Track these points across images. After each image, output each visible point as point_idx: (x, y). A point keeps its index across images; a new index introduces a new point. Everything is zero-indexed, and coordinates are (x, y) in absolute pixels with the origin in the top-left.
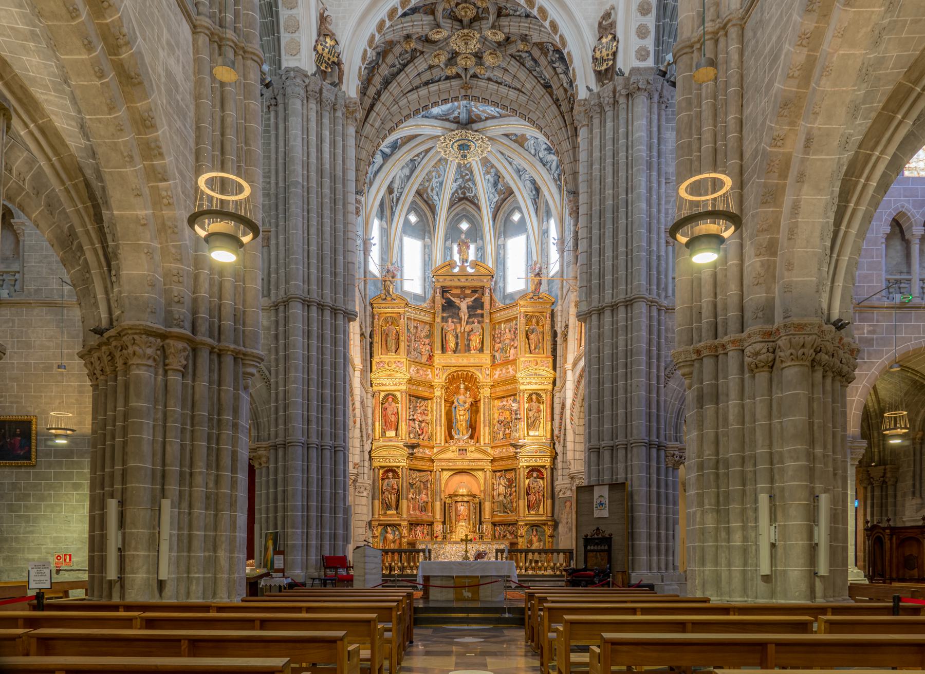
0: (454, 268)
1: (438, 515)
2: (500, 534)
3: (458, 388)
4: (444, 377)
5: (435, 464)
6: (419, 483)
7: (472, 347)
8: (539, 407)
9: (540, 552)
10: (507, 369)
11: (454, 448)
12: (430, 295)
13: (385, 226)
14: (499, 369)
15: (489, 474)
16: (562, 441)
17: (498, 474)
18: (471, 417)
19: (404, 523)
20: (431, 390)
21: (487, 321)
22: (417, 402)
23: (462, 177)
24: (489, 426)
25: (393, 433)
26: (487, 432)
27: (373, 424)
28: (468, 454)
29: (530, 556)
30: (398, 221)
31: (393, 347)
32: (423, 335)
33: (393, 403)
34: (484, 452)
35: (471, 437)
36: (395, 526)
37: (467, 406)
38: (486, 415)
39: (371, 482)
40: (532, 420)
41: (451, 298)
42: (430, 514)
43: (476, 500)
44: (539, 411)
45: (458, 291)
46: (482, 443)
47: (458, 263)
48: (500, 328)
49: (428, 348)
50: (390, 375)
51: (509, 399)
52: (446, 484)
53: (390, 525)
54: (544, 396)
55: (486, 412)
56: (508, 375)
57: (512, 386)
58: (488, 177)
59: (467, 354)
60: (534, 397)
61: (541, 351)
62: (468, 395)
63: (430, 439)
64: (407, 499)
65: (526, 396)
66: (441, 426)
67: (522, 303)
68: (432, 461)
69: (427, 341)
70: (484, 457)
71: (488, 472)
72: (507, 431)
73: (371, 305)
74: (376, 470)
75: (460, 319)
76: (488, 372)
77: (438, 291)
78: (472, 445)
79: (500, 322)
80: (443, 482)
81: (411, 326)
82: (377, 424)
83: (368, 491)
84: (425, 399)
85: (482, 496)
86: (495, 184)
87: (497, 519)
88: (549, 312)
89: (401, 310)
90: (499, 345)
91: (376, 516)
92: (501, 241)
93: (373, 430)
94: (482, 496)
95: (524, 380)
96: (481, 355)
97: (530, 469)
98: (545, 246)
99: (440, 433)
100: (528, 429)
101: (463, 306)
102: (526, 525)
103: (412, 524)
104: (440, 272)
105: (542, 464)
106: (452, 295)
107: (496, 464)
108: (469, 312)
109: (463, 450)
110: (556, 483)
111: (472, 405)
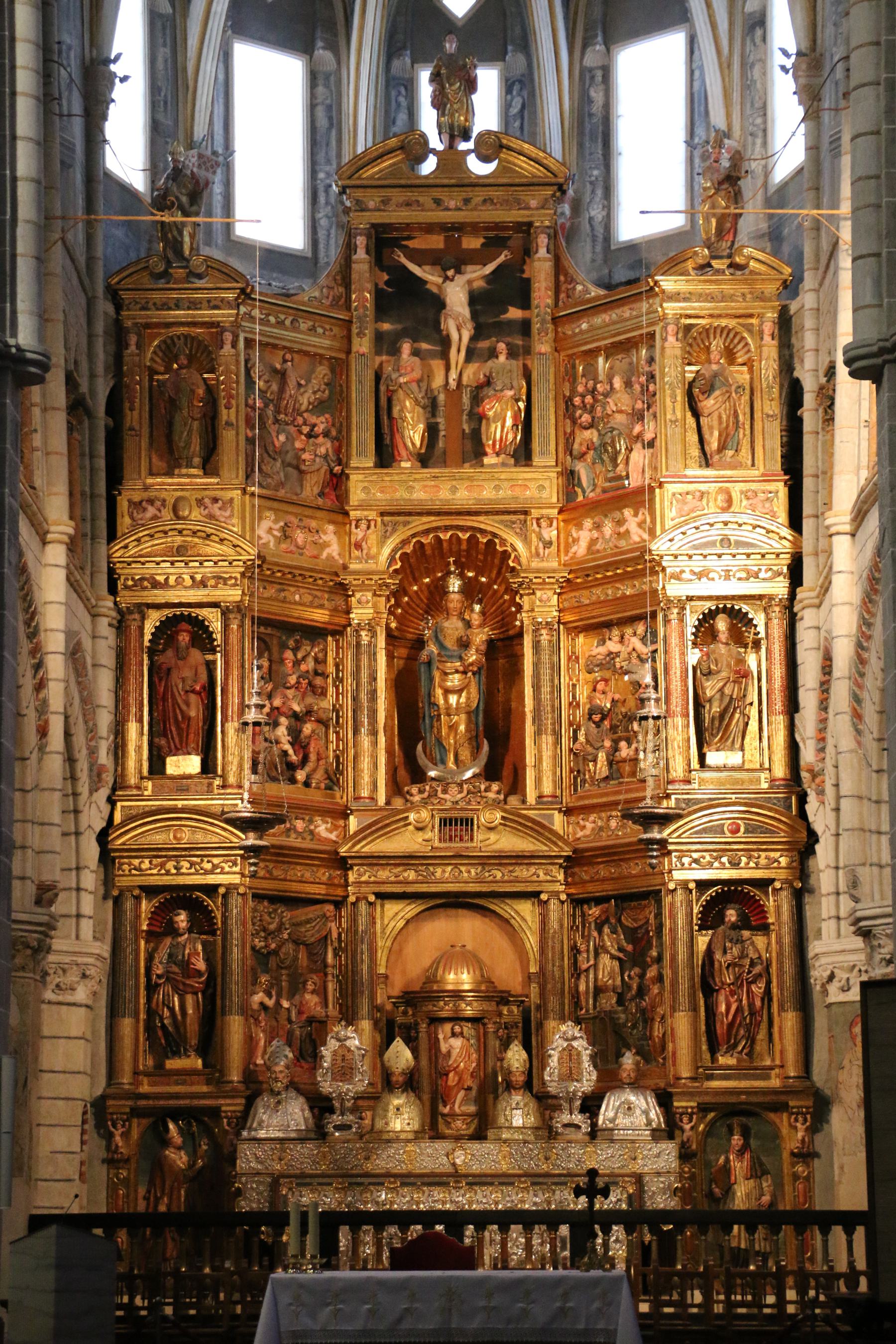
0: (422, 159)
3: (439, 591)
4: (386, 551)
5: (352, 877)
6: (290, 947)
8: (741, 661)
10: (620, 522)
11: (425, 814)
12: (331, 253)
14: (588, 523)
16: (830, 791)
17: (594, 911)
18: (489, 695)
20: (340, 602)
22: (283, 646)
25: (191, 764)
26: (547, 754)
28: (479, 836)
31: (196, 446)
33: (196, 656)
34: (539, 829)
35: (491, 773)
37: (472, 657)
38: (546, 689)
39: (105, 949)
40: (716, 709)
44: (743, 675)
45: (437, 242)
46: (531, 796)
47: (436, 143)
48: (591, 373)
49: (325, 446)
50: (181, 551)
51: (629, 631)
52: (396, 952)
53: (176, 1114)
54: (759, 619)
55: (545, 678)
56: (622, 543)
59: (467, 470)
60: (722, 624)
61: (745, 451)
63: (333, 780)
64: (245, 1011)
65: (691, 620)
66: (374, 733)
67: (668, 283)
68: (343, 864)
69: (321, 423)
71: (553, 905)
72: (625, 751)
73: (113, 294)
74: (129, 904)
75: (446, 342)
76: (551, 534)
77: (361, 241)
78: (496, 804)
79: (593, 353)
80: (382, 944)
82: (132, 728)
83: (92, 984)
88: (772, 315)
89: (224, 315)
90: (587, 434)
91: (126, 1079)
92: (592, 58)
93: (119, 749)
95: (683, 562)
96: (523, 473)
97: (712, 891)
100: (701, 744)
102: (703, 1109)
107: (584, 873)
108: (474, 315)
110: (814, 948)
111: (491, 648)
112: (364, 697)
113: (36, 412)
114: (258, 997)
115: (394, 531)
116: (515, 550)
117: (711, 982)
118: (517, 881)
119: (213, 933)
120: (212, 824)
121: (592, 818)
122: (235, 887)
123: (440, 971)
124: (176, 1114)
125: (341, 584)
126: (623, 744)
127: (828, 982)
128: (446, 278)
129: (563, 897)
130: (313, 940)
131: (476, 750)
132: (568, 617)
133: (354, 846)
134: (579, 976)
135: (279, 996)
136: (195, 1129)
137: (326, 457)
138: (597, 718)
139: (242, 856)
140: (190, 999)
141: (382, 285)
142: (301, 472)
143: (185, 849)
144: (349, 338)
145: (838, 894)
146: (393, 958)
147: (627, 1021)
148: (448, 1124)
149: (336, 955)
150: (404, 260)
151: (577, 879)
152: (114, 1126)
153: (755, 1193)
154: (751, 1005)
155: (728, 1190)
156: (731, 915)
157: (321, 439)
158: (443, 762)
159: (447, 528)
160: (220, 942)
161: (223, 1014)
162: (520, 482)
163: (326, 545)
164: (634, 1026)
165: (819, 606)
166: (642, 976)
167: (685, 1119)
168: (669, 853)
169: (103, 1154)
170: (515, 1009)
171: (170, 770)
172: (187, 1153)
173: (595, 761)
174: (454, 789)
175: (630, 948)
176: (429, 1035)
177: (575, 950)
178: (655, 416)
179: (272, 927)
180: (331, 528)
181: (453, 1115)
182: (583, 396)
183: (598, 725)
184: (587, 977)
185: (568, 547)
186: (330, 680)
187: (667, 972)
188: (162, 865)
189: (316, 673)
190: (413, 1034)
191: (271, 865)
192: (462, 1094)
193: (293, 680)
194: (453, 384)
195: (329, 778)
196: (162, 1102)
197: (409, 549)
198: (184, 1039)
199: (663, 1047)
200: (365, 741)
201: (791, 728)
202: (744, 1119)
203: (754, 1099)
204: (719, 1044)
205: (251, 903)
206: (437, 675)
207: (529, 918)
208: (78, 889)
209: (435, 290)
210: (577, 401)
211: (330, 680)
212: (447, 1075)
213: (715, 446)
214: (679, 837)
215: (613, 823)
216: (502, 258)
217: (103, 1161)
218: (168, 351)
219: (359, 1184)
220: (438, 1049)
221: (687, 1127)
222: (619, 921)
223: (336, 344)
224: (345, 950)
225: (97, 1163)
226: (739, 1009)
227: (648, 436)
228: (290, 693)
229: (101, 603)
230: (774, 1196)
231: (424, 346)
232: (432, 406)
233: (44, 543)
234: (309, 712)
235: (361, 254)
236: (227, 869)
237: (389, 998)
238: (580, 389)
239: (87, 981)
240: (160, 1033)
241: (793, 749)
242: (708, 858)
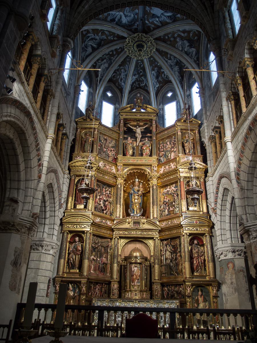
1: (115, 276)
2: (168, 294)
5: (114, 233)
7: (144, 154)
9: (208, 312)
13: (92, 91)
14: (163, 167)
15: (158, 242)
17: (165, 242)
19: (84, 281)
21: (154, 138)
22: (103, 187)
23: (139, 74)
24: (157, 205)
25: (82, 206)
27: (67, 200)
29: (198, 316)
30: (100, 90)
32: (110, 145)
34: (154, 224)
35: (143, 215)
36: (77, 284)
37: (140, 193)
38: (155, 197)
39: (59, 244)
41: (132, 127)
42: (108, 274)
43: (147, 263)
45: (135, 123)
46: (152, 218)
49: (114, 153)
51: (172, 186)
53: (71, 282)
56: (170, 169)
57: (174, 176)
58: (153, 72)
62: (141, 186)
63: (111, 214)
64: (89, 259)
68: (112, 230)
70: (155, 228)
71: (157, 239)
72: (171, 209)
74: (65, 234)
77: (122, 121)
81: (102, 139)
82: (70, 199)
84: (110, 186)
85: (152, 260)
86: (157, 77)
87: (165, 280)
90: (162, 153)
91: (61, 273)
94: (152, 260)
98: (189, 102)
99: (119, 212)
101: (139, 131)
102: (192, 285)
103: (92, 282)
104: (124, 111)
105: (202, 232)
106: (131, 125)
107: (163, 234)
108: (142, 134)
109: (137, 223)
112: (118, 197)
113: (49, 113)
114: (92, 257)
115: (126, 169)
116: (149, 173)
117: (192, 256)
118: (149, 235)
119: (83, 243)
120: (85, 218)
121: (165, 222)
122: (89, 231)
123: (132, 252)
124: (71, 282)
125: (115, 176)
126: (171, 208)
127: (220, 255)
128: (137, 128)
129: (159, 238)
130: (105, 246)
131: (140, 211)
132: (158, 185)
133: (115, 226)
134: (162, 256)
135: (97, 257)
136: (75, 286)
137: (113, 155)
138: (165, 203)
139: (91, 225)
140: (77, 256)
141: (125, 130)
142: (109, 157)
143: (78, 223)
144: (119, 136)
145: (222, 235)
146: (122, 251)
147: (173, 266)
148: (133, 287)
149: (110, 250)
150: (129, 126)
151: (161, 235)
152: (57, 284)
153: (205, 306)
154: (201, 261)
155: (198, 304)
156: (196, 242)
157: (113, 151)
158: (134, 213)
159: (136, 169)
160: (84, 245)
161: (84, 259)
162: (150, 160)
163: (113, 169)
164: (174, 267)
165: (212, 177)
166: (176, 256)
167: (188, 287)
168: (183, 227)
169: (54, 291)
170: (148, 262)
171: (77, 207)
172: (73, 292)
173: (165, 212)
174: (136, 218)
175: (173, 250)
176: (130, 267)
177: (161, 250)
178: (176, 147)
179: (96, 242)
180: (114, 167)
181: (134, 285)
182: (161, 147)
183: (165, 205)
184: (164, 256)
185: (159, 172)
186: (112, 195)
187: (183, 254)
188: (73, 226)
189: (109, 194)
190: (126, 267)
191: (97, 228)
192: (137, 280)
193: (104, 193)
194: (138, 145)
195: (111, 213)
196: (68, 279)
197: (128, 173)
198: (75, 266)
199: (182, 271)
200: (118, 206)
201: (207, 202)
202: (201, 288)
203: (204, 283)
204: (194, 271)
205: (92, 236)
206: (133, 196)
207: (151, 243)
208: (54, 229)
209: (135, 131)
210: (160, 148)
211: (112, 195)
212: (133, 276)
213: (188, 152)
214: (185, 223)
215: (169, 223)
216: (147, 126)
217: (54, 293)
218: (86, 134)
219: (112, 301)
220: (132, 270)
221: (189, 289)
222: (171, 244)
223: (117, 137)
224: (112, 249)
225: (52, 293)
226: (199, 262)
227: (175, 150)
228: (104, 196)
229: (66, 171)
230: (209, 307)
231: (133, 139)
232: (134, 149)
233: (47, 139)
234: (107, 201)
235: (122, 123)
236: (87, 227)
237: (121, 259)
238: (161, 146)
239: (53, 249)
240: (70, 264)
241: (207, 207)
242: (191, 228)
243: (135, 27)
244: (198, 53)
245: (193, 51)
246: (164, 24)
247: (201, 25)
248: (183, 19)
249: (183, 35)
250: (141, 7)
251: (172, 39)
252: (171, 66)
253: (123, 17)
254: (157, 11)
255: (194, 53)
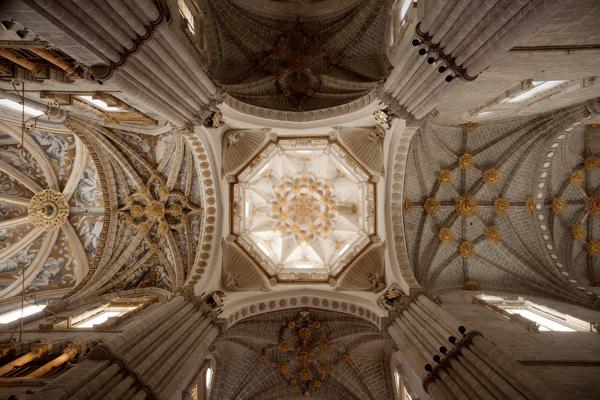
243: (77, 203)
244: (41, 289)
245: (43, 282)
246: (82, 239)
247: (83, 284)
248: (89, 261)
249: (68, 264)
250: (103, 210)
251: (61, 252)
252: (17, 256)
253: (91, 188)
254: (98, 228)
255: (41, 284)
